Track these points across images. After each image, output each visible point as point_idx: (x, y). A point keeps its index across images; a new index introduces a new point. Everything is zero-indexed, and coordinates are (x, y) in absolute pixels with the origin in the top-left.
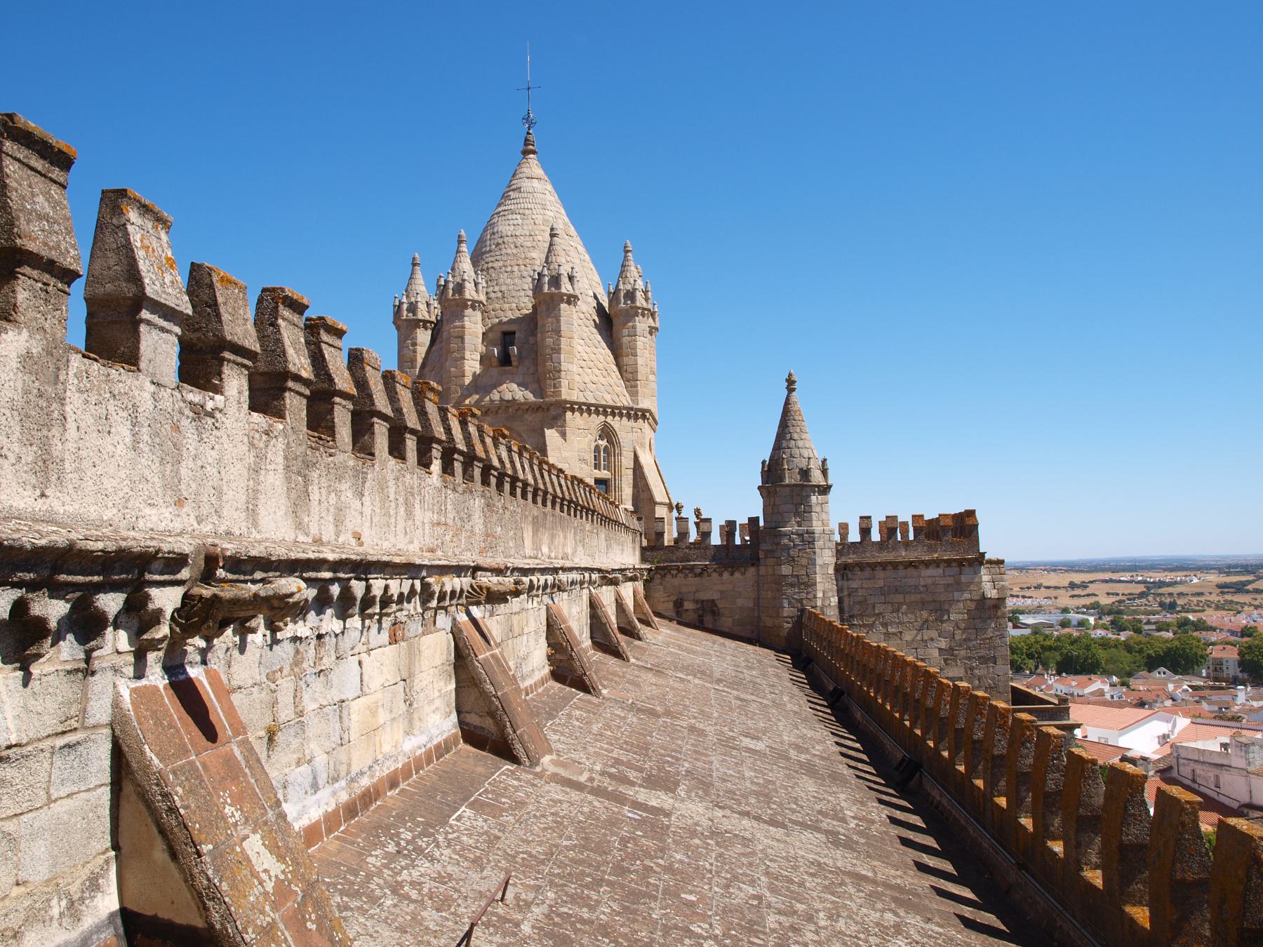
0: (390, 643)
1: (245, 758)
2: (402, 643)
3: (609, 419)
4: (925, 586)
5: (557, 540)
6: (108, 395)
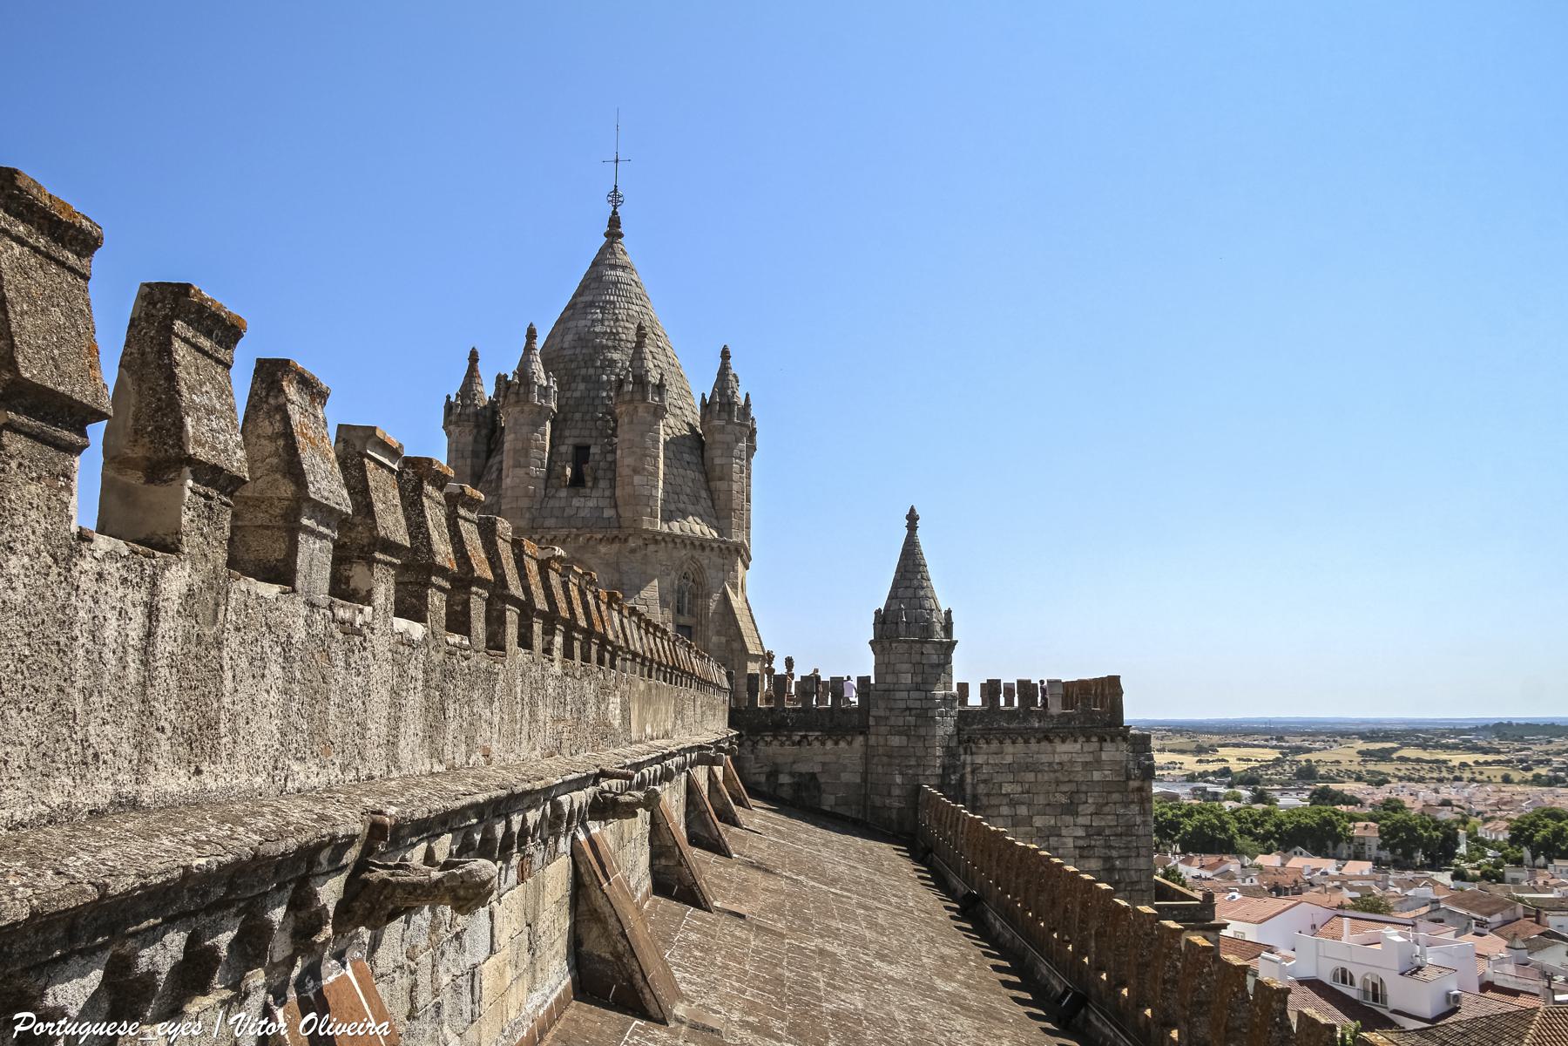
0: (518, 884)
2: (529, 880)
3: (697, 554)
4: (1060, 763)
6: (264, 629)
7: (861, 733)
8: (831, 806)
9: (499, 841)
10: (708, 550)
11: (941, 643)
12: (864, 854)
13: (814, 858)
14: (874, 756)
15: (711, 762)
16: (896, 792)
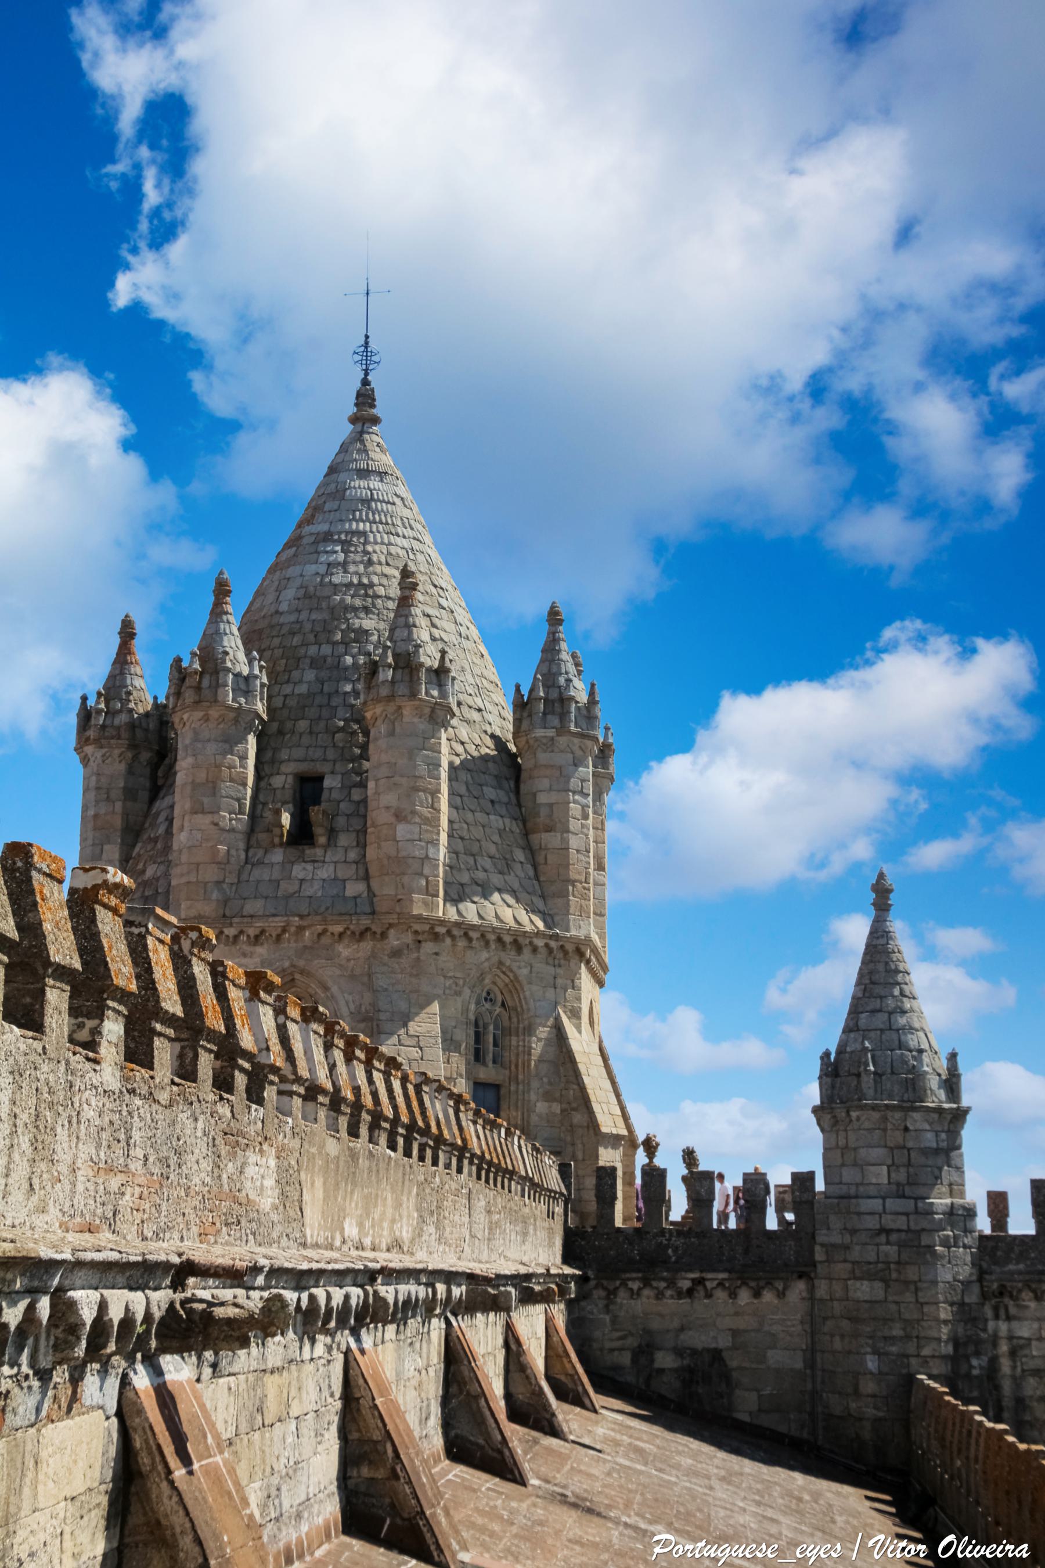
3: (509, 958)
5: (380, 1208)
7: (800, 1277)
8: (751, 1413)
10: (527, 952)
11: (939, 1111)
12: (800, 1500)
13: (694, 1498)
14: (825, 1319)
15: (496, 1305)
16: (869, 1387)
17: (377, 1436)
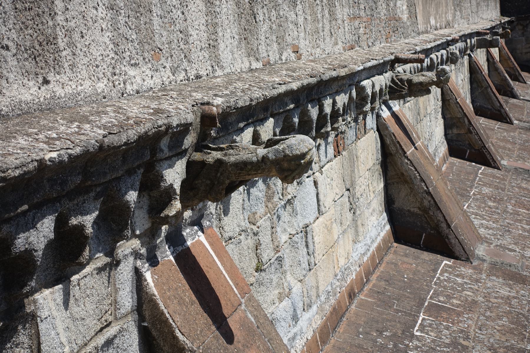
0: (335, 156)
1: (256, 317)
2: (344, 153)
5: (441, 8)
9: (315, 122)
15: (486, 45)
17: (459, 115)
